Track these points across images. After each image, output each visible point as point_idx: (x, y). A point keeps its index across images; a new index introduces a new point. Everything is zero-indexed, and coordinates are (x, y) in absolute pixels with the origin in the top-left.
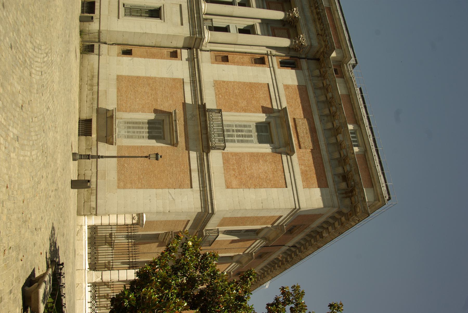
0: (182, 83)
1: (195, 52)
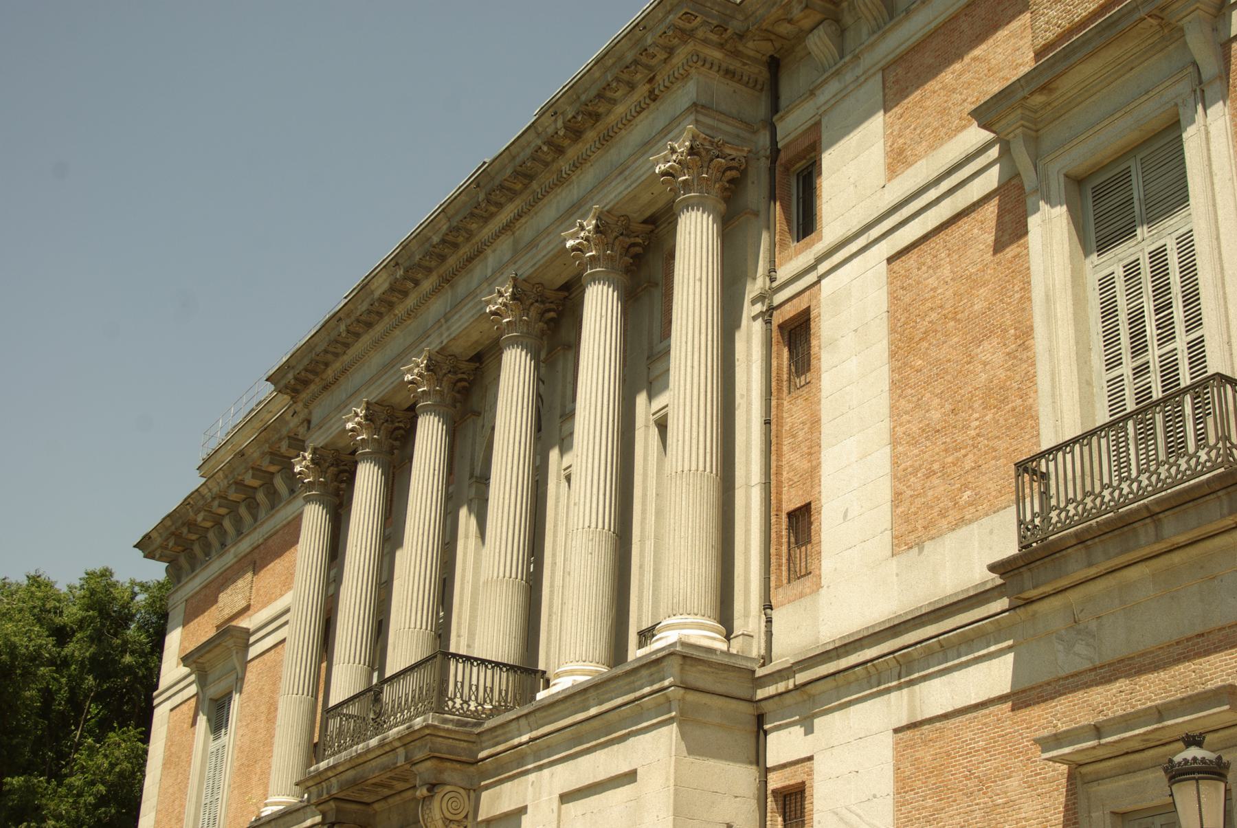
1: (771, 690)
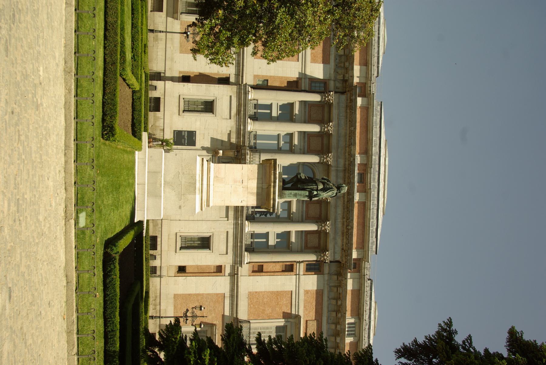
0: (223, 297)
